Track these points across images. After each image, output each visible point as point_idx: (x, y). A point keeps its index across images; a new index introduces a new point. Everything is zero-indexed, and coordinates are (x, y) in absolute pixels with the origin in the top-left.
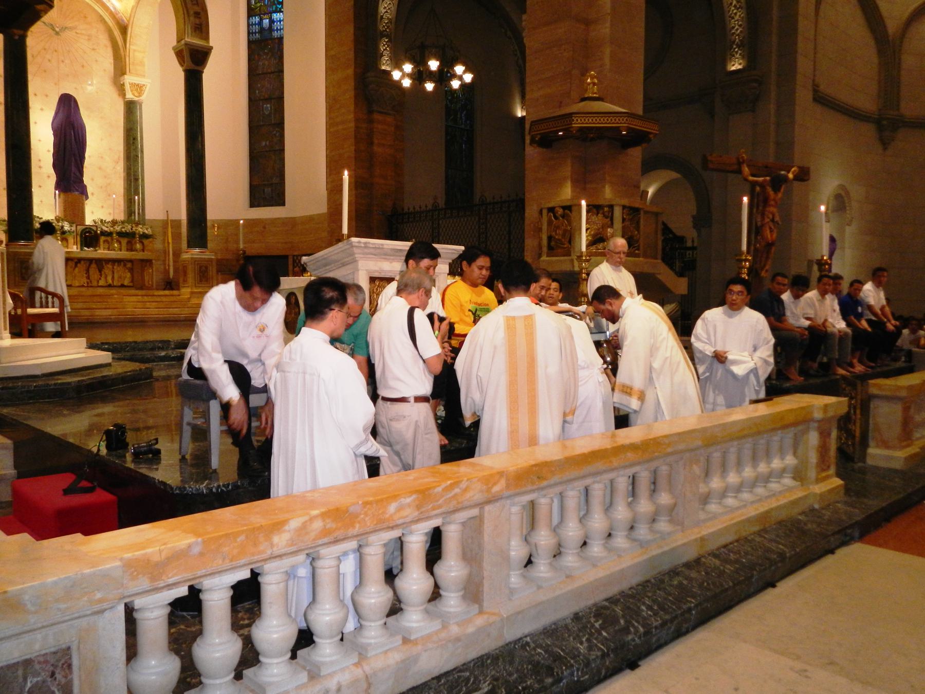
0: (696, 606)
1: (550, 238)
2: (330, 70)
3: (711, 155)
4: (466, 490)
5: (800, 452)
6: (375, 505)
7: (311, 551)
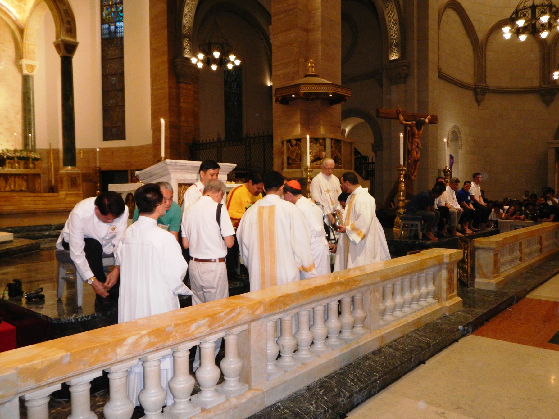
0: (379, 378)
1: (288, 158)
2: (153, 57)
4: (239, 314)
5: (437, 283)
6: (182, 326)
7: (142, 357)
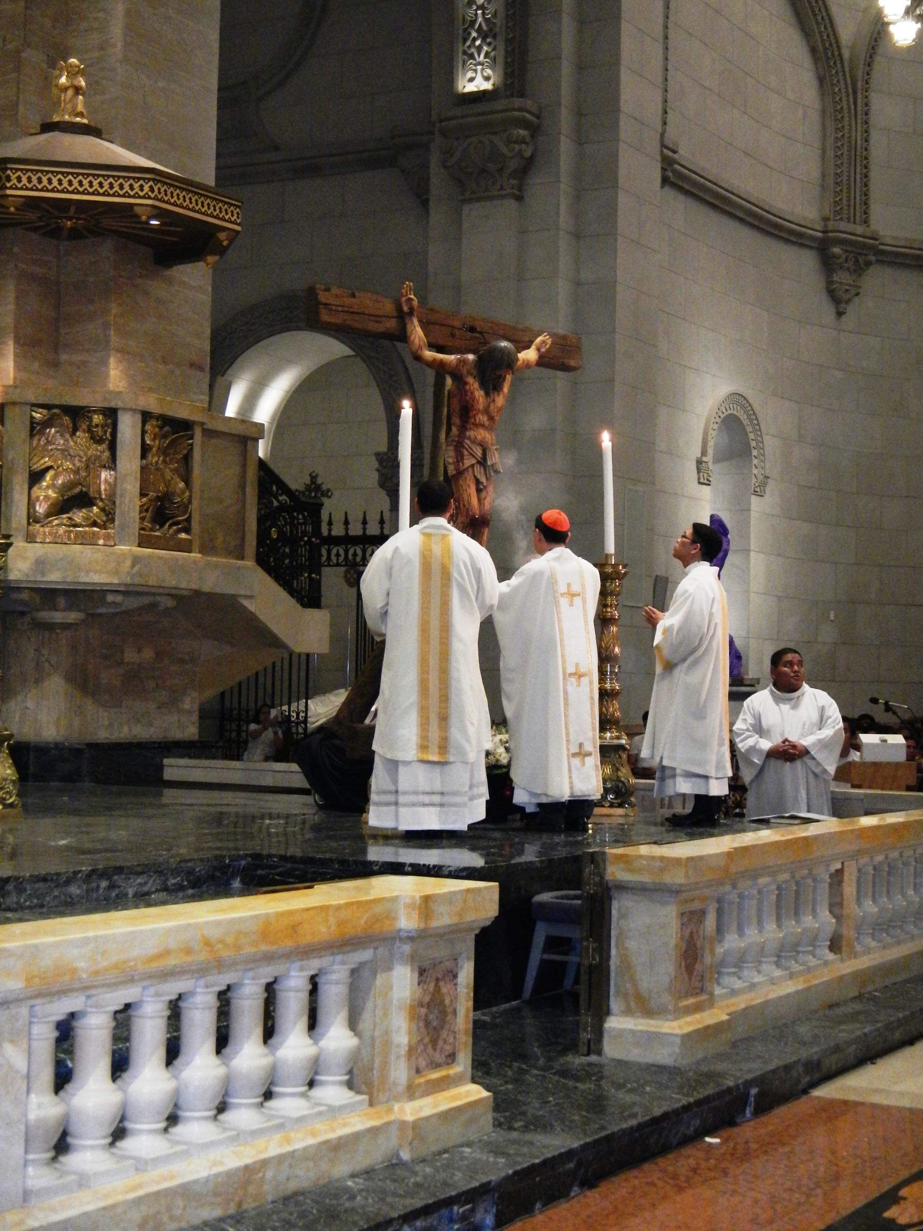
3: (328, 290)
